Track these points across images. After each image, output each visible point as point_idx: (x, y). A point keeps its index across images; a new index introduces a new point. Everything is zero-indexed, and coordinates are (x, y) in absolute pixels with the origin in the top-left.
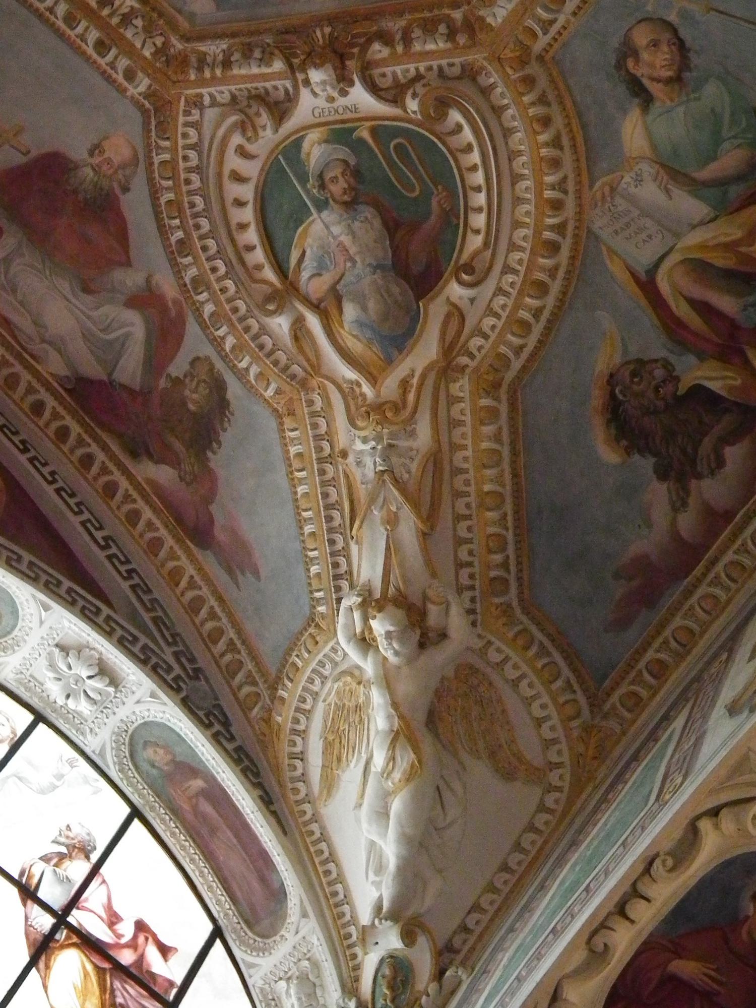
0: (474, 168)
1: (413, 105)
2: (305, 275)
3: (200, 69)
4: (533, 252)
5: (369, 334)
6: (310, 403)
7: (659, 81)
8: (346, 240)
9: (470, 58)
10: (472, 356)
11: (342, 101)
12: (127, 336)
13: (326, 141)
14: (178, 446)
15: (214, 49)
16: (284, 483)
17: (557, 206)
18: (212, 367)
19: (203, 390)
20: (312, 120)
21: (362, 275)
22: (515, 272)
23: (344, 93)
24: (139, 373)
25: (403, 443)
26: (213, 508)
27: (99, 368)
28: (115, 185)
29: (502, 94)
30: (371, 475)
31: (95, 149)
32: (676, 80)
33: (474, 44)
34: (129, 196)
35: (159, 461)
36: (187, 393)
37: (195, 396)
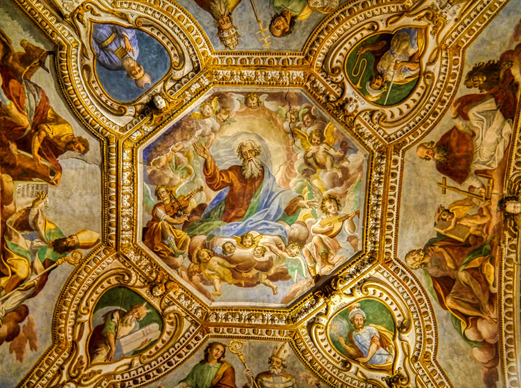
0: (345, 49)
1: (339, 78)
2: (413, 73)
3: (377, 144)
4: (355, 15)
5: (413, 41)
6: (450, 43)
7: (286, 19)
8: (392, 68)
9: (316, 72)
10: (397, 7)
11: (354, 98)
12: (479, 113)
13: (369, 94)
14: (501, 75)
15: (370, 144)
16: (484, 32)
17: (338, 19)
18: (466, 81)
19: (476, 78)
20: (366, 103)
21: (398, 56)
22: (365, 15)
23: (351, 99)
24: (488, 101)
25: (437, 5)
26: (513, 48)
27: (497, 115)
28: (434, 146)
29: (320, 57)
30: (455, 7)
31: (427, 159)
32: (283, 14)
33: (312, 74)
34: (433, 140)
35: (512, 76)
36: (481, 83)
37: (480, 80)
